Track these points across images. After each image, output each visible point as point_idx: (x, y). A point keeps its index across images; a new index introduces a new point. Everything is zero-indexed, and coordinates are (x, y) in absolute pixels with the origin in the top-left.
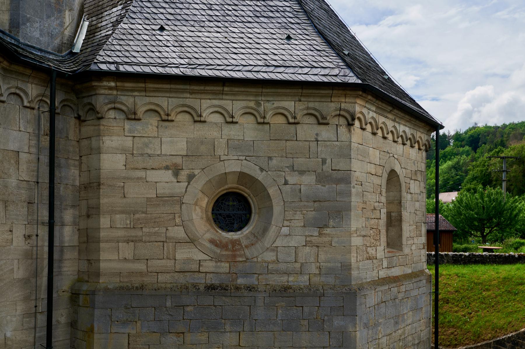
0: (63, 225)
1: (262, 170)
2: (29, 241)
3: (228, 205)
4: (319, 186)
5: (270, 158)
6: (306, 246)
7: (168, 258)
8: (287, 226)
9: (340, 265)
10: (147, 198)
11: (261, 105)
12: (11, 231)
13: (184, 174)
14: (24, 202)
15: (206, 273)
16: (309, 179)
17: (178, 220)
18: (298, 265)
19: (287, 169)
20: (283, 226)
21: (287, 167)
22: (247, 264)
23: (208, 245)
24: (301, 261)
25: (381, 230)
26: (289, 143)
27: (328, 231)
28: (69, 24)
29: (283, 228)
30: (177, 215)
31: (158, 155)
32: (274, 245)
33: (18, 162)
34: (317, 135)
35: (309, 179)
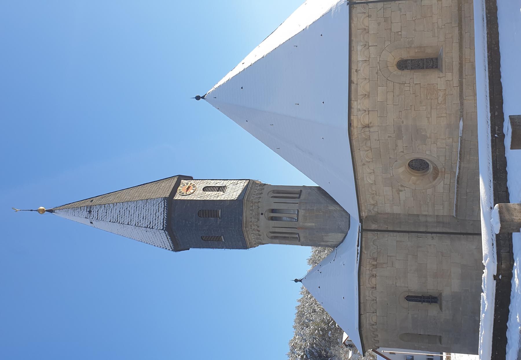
0: (427, 222)
1: (396, 161)
2: (434, 238)
3: (415, 164)
4: (403, 139)
5: (390, 158)
6: (437, 144)
7: (443, 194)
8: (426, 152)
9: (448, 129)
10: (413, 200)
11: (364, 163)
12: (430, 245)
13: (400, 188)
14: (417, 239)
15: (450, 182)
16: (400, 143)
17: (423, 191)
18: (447, 147)
19: (395, 151)
20: (426, 153)
21: (394, 152)
22: (446, 167)
23: (436, 181)
24: (445, 146)
25: (428, 83)
26: (381, 151)
27: (428, 135)
28: (334, 207)
29: (427, 153)
30: (421, 191)
31: (393, 196)
32: (436, 157)
33: (401, 241)
34: (375, 140)
35: (400, 143)
